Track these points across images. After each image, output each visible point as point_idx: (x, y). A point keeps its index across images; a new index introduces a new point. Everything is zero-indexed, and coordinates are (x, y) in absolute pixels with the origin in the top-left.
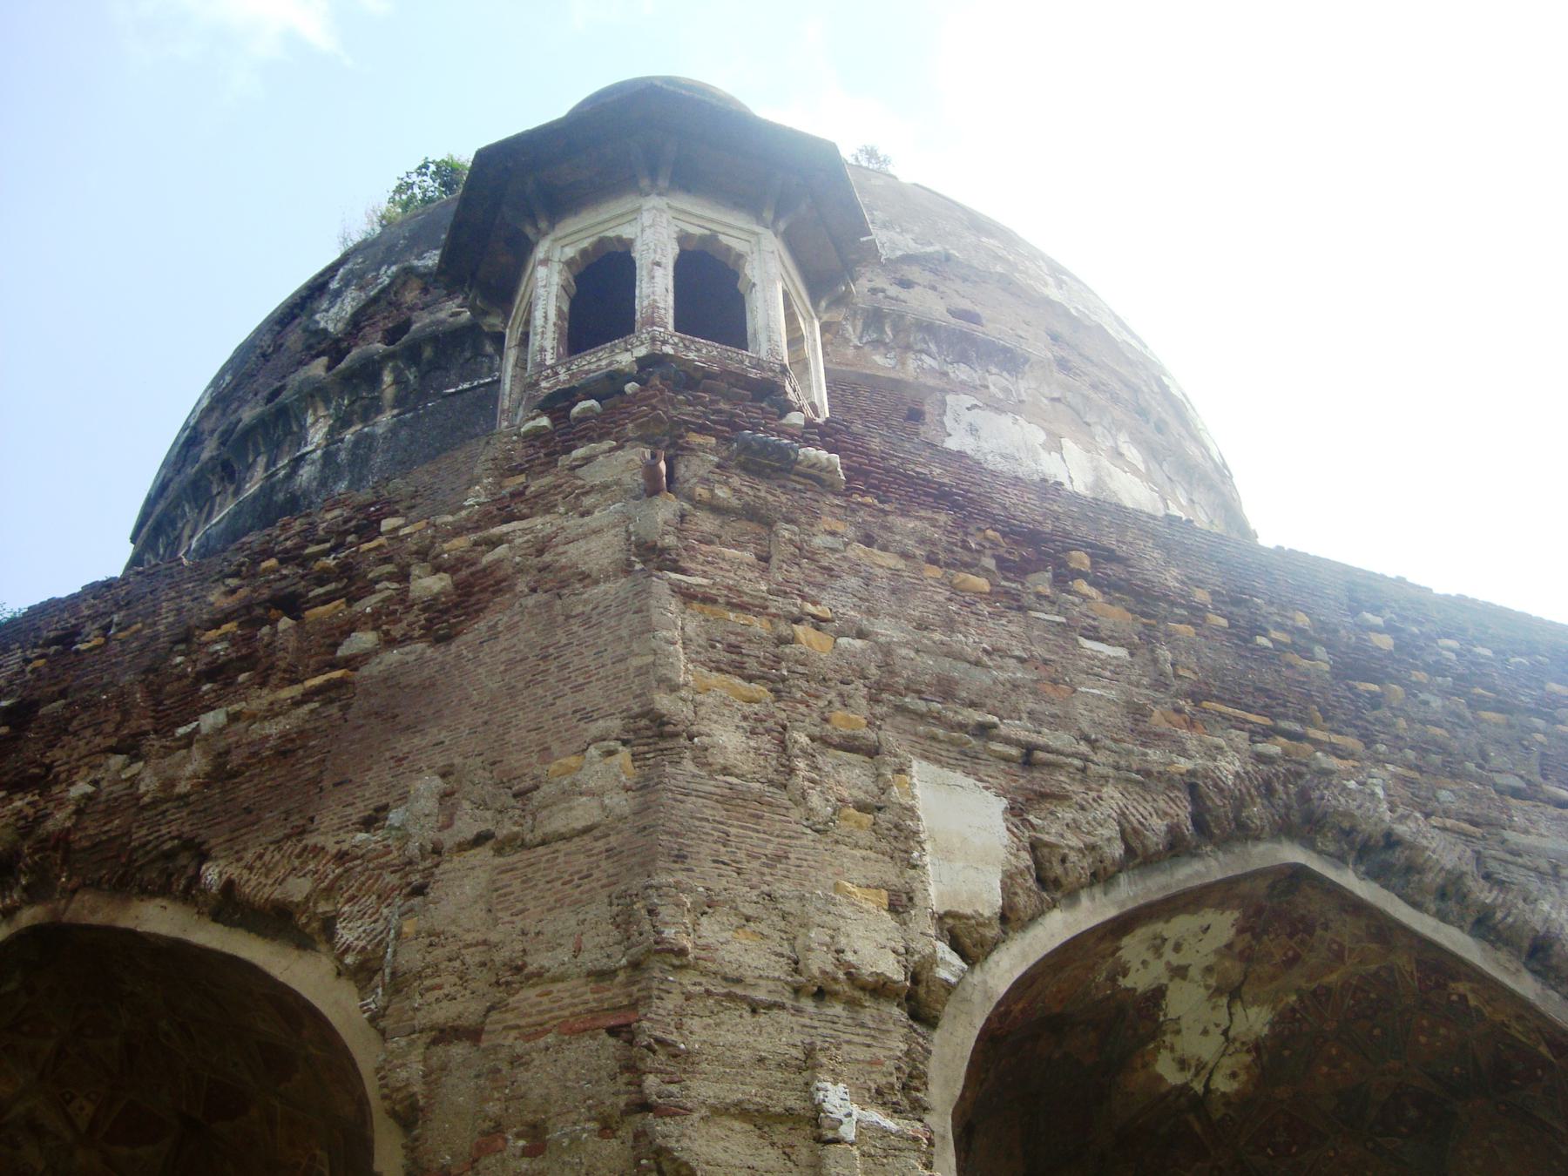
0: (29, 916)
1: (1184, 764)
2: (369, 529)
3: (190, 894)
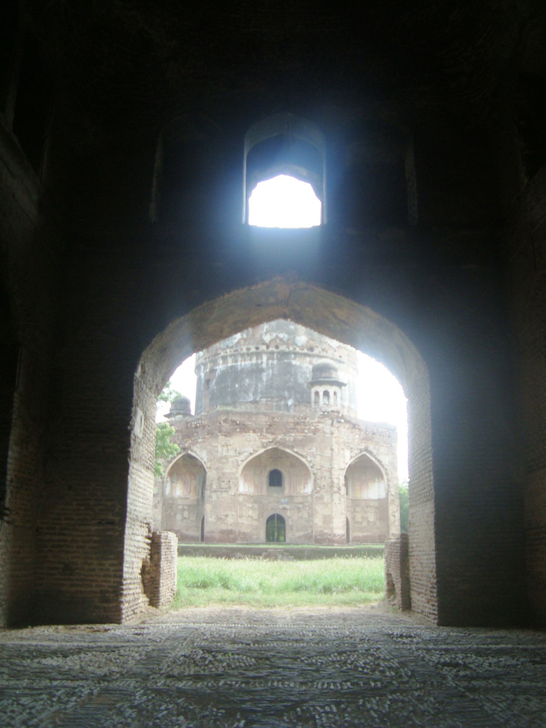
0: (274, 446)
1: (360, 447)
2: (305, 418)
3: (292, 450)
